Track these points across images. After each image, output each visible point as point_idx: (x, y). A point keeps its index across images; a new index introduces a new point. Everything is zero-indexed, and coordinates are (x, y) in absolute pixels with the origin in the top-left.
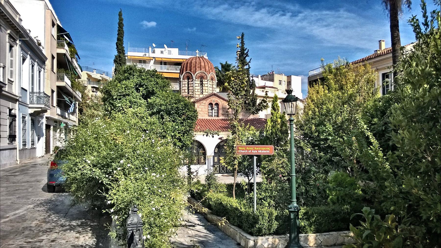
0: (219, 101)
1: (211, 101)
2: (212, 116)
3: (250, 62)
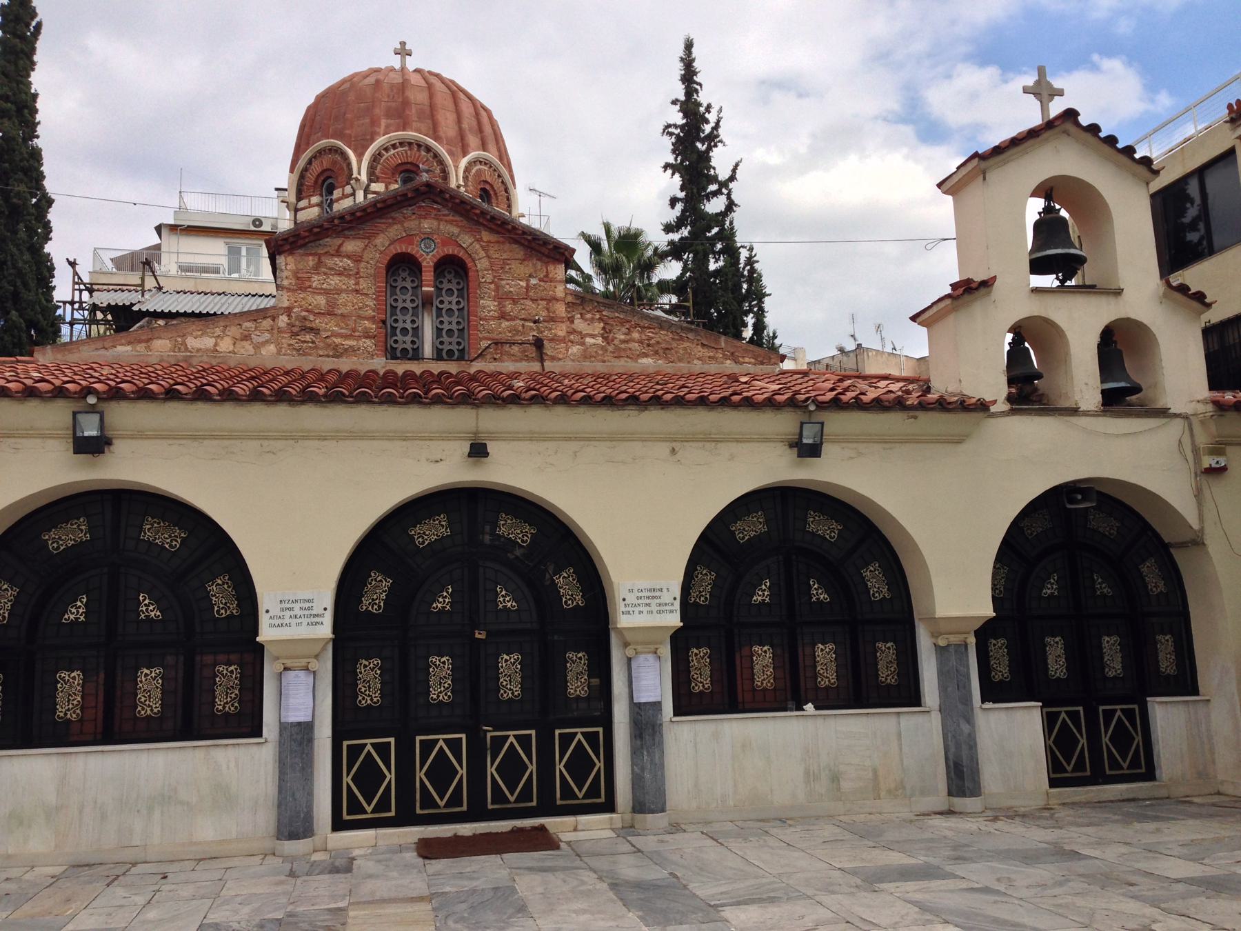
0: (466, 240)
1: (409, 238)
2: (416, 355)
3: (732, 178)
